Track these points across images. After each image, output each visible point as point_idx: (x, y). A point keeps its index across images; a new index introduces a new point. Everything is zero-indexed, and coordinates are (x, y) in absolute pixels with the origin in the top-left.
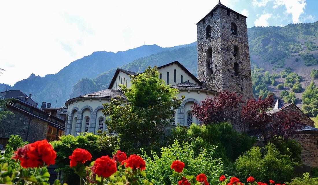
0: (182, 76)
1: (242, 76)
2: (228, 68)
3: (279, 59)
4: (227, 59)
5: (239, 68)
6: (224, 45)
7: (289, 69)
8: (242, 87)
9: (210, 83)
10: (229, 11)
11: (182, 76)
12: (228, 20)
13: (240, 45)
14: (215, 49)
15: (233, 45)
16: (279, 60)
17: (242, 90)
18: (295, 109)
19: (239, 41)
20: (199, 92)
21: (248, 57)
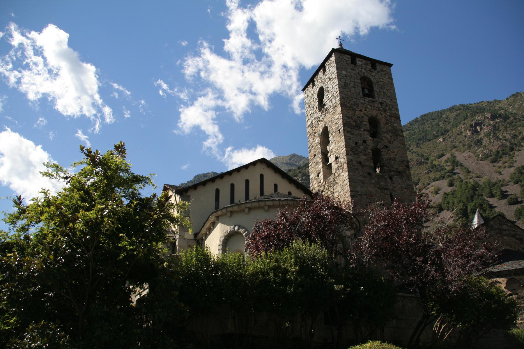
0: (276, 186)
1: (391, 171)
2: (359, 160)
3: (504, 154)
4: (356, 143)
5: (383, 157)
6: (348, 117)
10: (354, 57)
11: (276, 186)
12: (353, 72)
13: (382, 115)
14: (334, 128)
15: (367, 116)
16: (504, 156)
18: (507, 225)
19: (379, 108)
21: (400, 136)
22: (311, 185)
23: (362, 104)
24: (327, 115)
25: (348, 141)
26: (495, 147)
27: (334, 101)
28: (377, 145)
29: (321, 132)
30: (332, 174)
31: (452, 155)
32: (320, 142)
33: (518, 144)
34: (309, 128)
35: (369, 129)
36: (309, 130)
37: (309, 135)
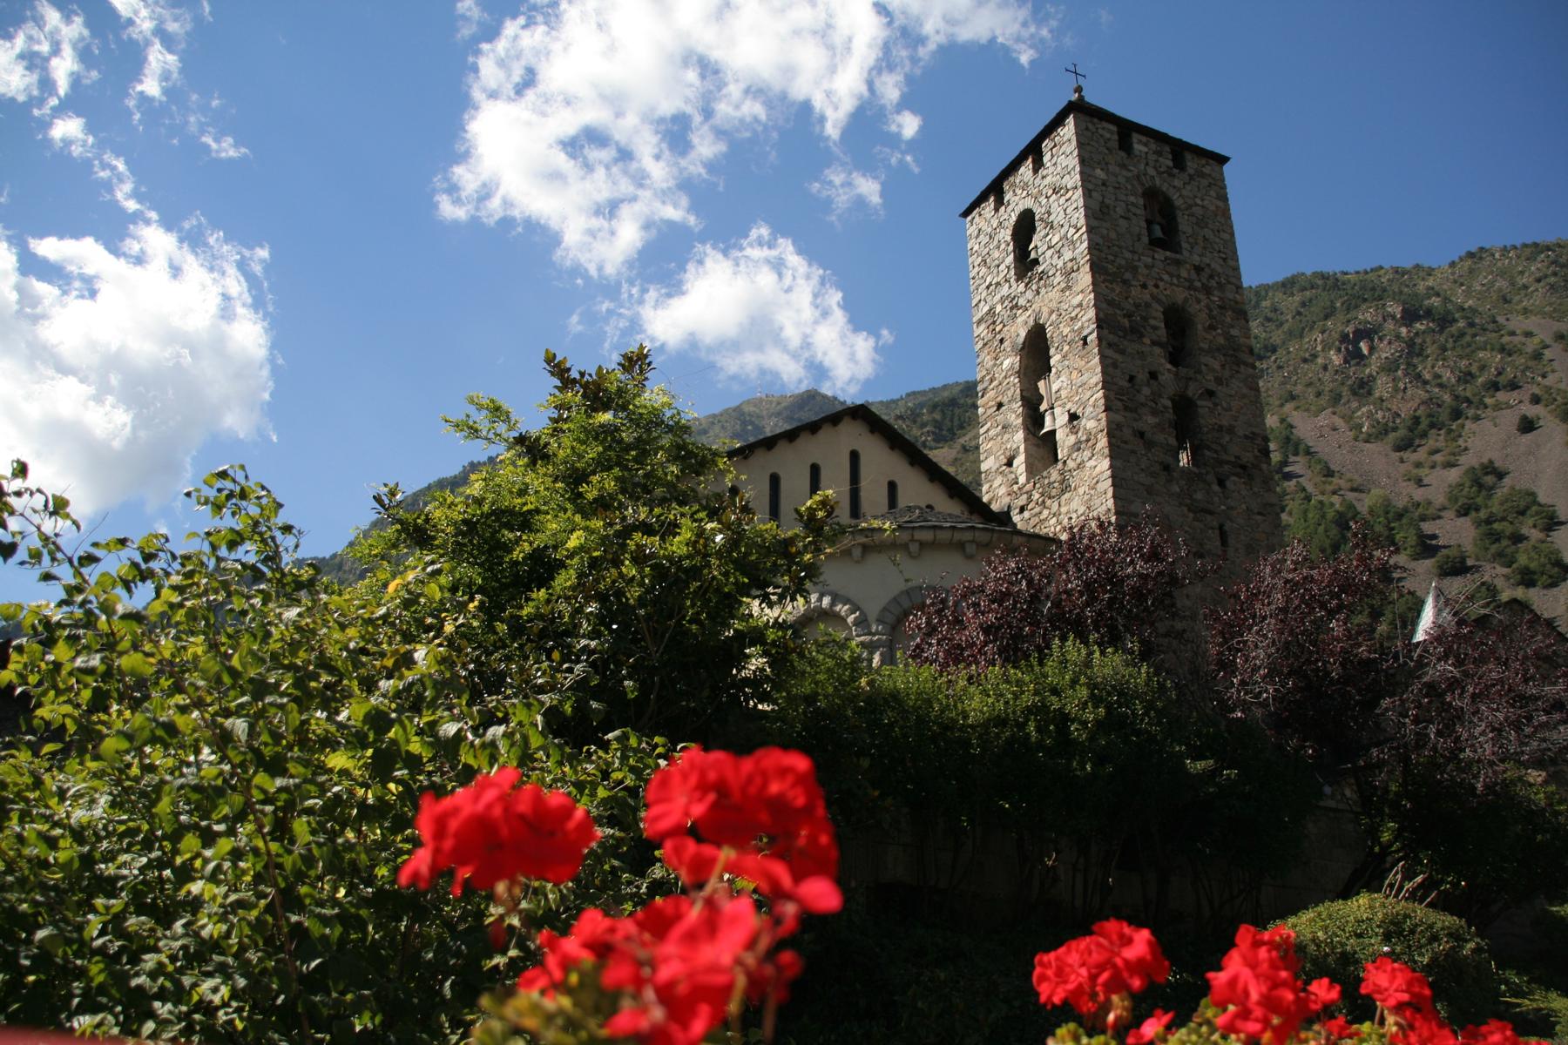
0: (892, 486)
1: (1221, 463)
2: (1139, 425)
3: (1432, 426)
4: (1132, 379)
6: (1111, 303)
7: (1487, 474)
8: (1221, 527)
9: (1046, 512)
10: (1127, 130)
11: (892, 486)
12: (1124, 172)
13: (1199, 301)
14: (1066, 331)
15: (1159, 301)
16: (1433, 431)
17: (1224, 542)
19: (1190, 281)
20: (971, 549)
21: (1246, 364)
22: (985, 488)
23: (1146, 266)
24: (1043, 291)
25: (1110, 370)
26: (1409, 404)
28: (1186, 387)
29: (1021, 339)
30: (1056, 460)
31: (1283, 421)
32: (1017, 366)
33: (1475, 400)
34: (983, 326)
35: (1164, 340)
36: (981, 330)
37: (980, 344)
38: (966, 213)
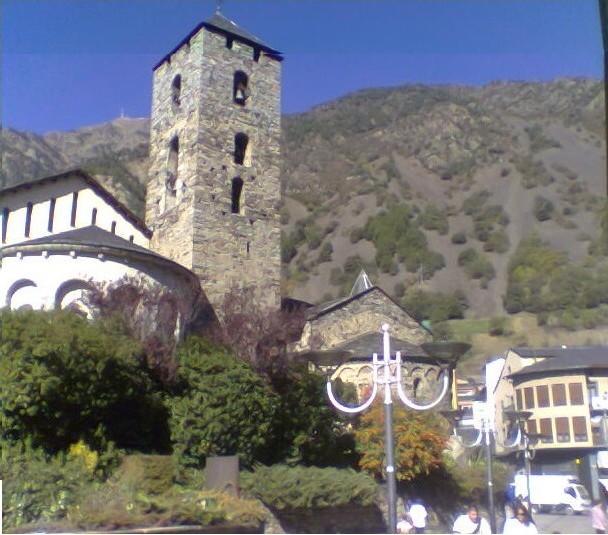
4: (212, 169)
11: (95, 211)
15: (234, 131)
27: (192, 101)
38: (155, 69)
